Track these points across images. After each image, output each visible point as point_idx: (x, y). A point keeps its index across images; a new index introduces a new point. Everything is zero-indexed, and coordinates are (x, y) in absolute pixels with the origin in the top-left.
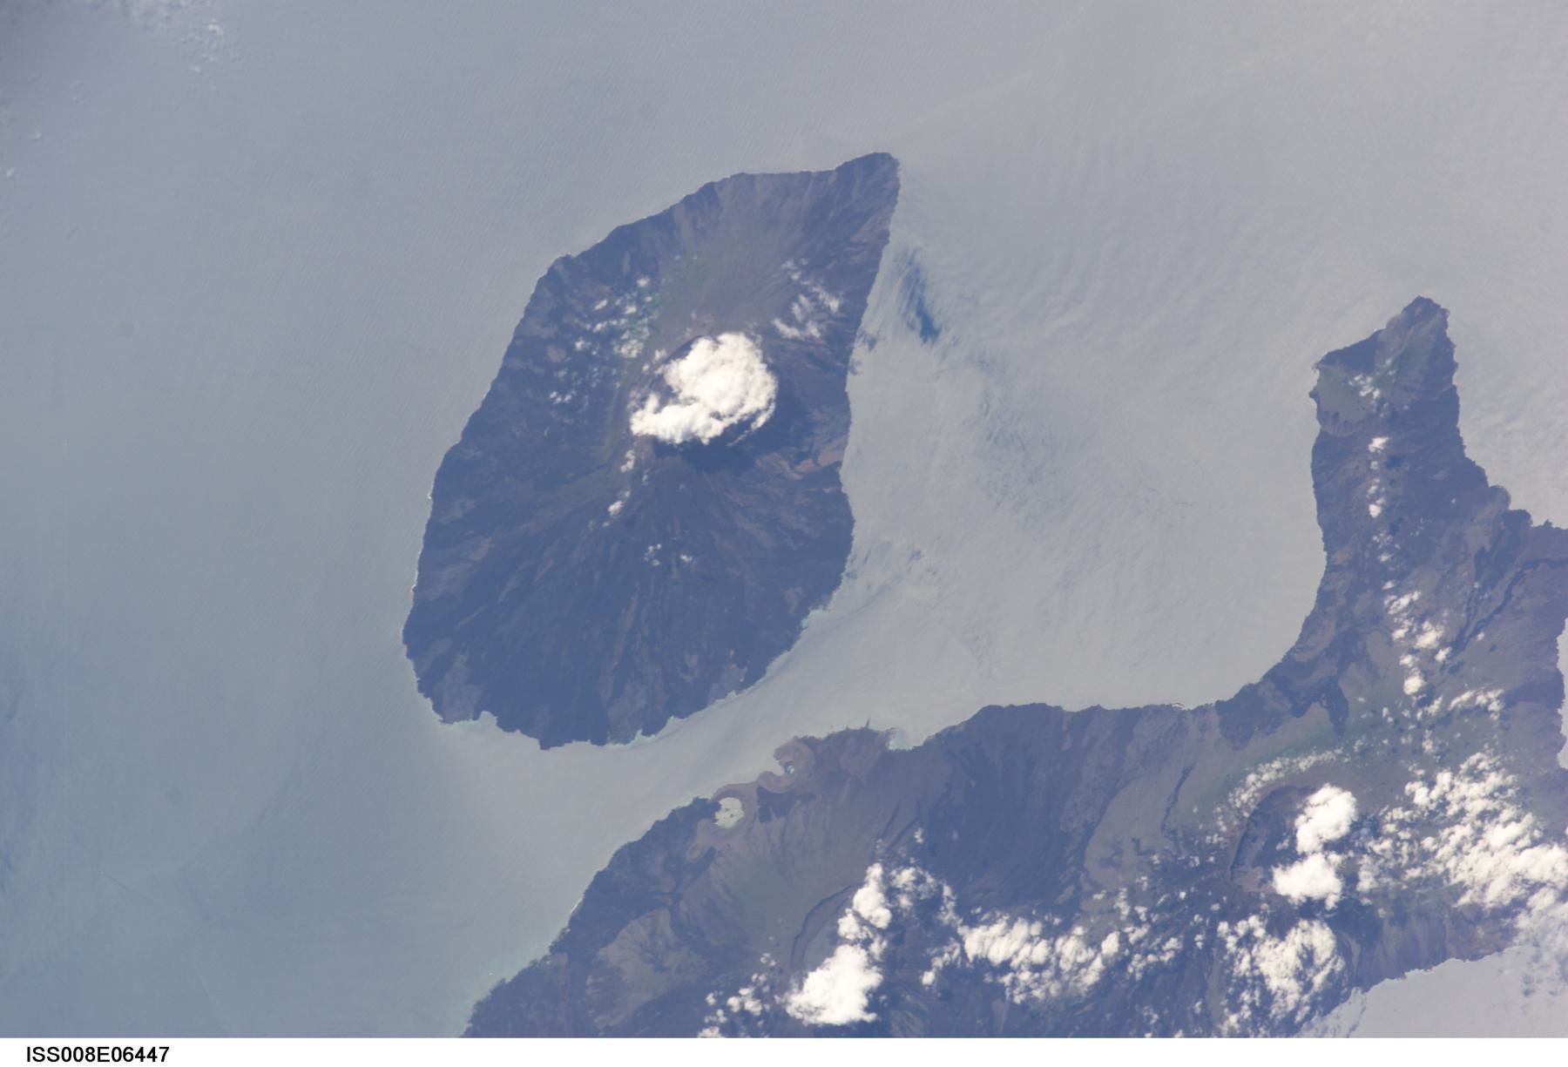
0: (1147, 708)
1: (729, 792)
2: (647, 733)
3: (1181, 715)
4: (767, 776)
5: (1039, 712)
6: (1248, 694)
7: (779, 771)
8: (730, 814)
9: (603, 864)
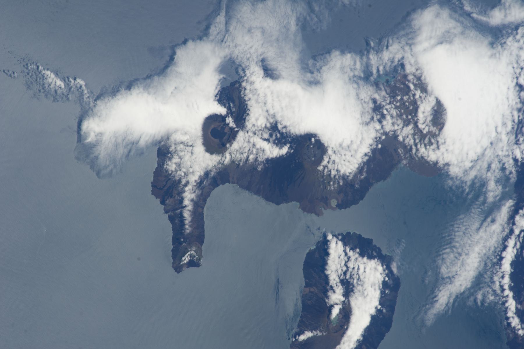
0: (244, 189)
1: (333, 209)
2: (350, 233)
3: (237, 184)
4: (325, 209)
5: (268, 198)
6: (223, 183)
7: (323, 209)
8: (334, 203)
9: (361, 201)
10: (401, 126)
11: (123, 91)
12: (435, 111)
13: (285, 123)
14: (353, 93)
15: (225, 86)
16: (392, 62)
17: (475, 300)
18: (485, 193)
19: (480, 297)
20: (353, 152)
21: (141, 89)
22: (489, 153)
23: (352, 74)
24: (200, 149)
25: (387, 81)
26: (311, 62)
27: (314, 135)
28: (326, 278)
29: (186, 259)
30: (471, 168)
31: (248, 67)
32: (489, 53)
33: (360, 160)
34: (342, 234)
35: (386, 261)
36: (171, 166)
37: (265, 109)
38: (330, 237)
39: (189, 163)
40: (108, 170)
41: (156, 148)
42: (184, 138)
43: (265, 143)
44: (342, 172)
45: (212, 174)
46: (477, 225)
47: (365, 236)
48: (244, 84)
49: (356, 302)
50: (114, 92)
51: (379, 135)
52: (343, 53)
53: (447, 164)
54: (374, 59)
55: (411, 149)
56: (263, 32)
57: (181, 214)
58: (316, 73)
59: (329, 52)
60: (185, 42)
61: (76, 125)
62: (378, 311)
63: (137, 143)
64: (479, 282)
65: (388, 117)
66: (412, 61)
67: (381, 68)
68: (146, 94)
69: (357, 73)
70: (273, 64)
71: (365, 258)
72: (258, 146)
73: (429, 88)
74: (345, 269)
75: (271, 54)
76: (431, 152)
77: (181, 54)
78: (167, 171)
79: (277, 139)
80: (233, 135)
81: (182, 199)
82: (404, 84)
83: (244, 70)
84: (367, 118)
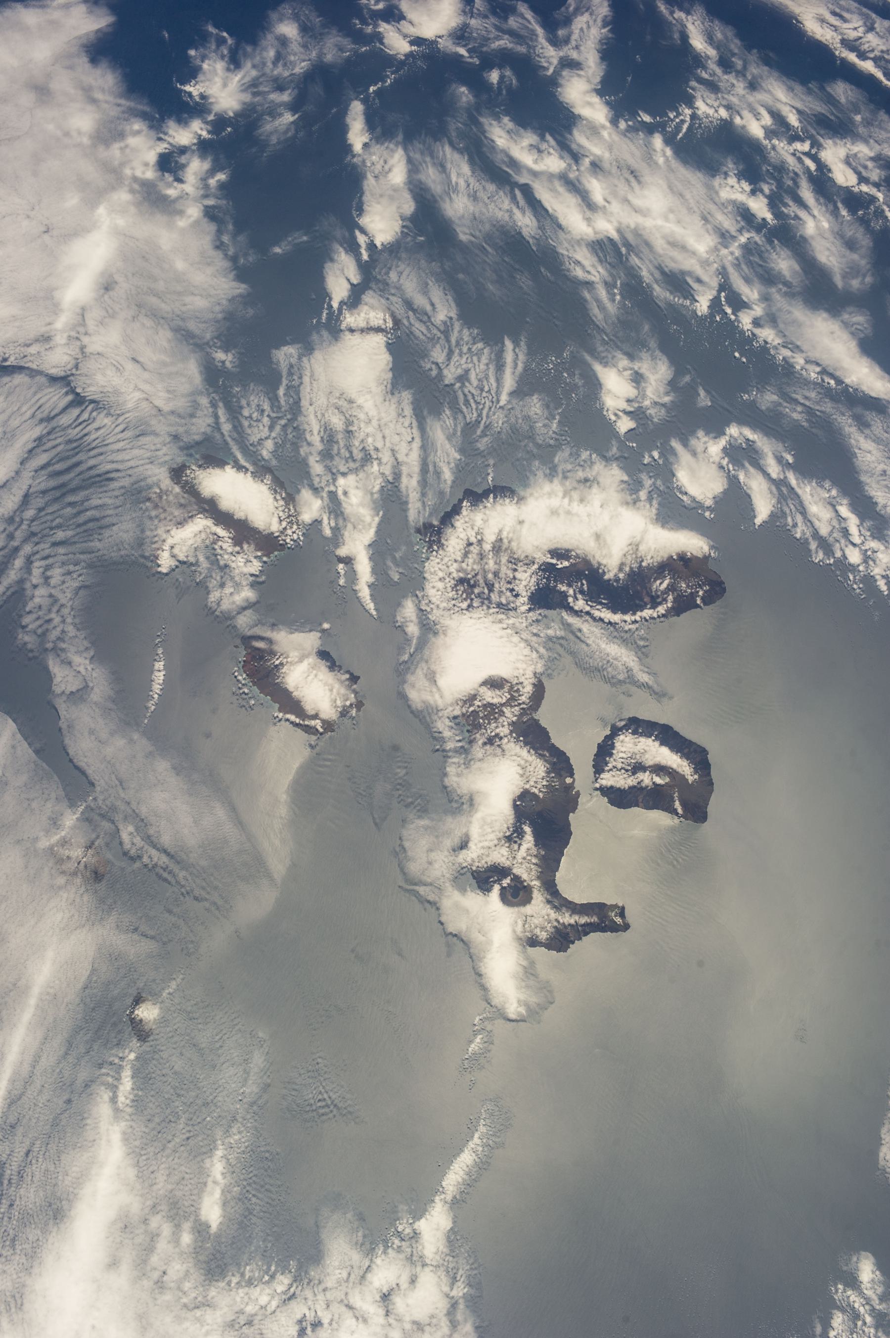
5: (567, 843)
6: (556, 885)
8: (569, 780)
10: (504, 718)
11: (483, 981)
12: (491, 686)
13: (505, 829)
14: (478, 764)
15: (476, 885)
16: (452, 728)
17: (644, 647)
18: (558, 638)
19: (642, 643)
20: (527, 764)
21: (482, 964)
22: (525, 635)
23: (463, 766)
24: (528, 909)
25: (468, 731)
26: (455, 805)
27: (515, 801)
28: (632, 788)
29: (618, 920)
30: (537, 652)
31: (460, 864)
32: (442, 636)
33: (534, 757)
34: (595, 773)
35: (615, 731)
36: (543, 936)
37: (493, 848)
38: (597, 785)
39: (541, 919)
40: (548, 994)
41: (528, 947)
42: (520, 923)
43: (522, 847)
44: (544, 774)
45: (548, 897)
46: (584, 646)
47: (595, 750)
48: (474, 868)
49: (649, 760)
50: (484, 988)
51: (512, 740)
52: (445, 775)
53: (535, 674)
54: (450, 745)
55: (522, 709)
56: (431, 850)
57: (582, 926)
58: (463, 800)
59: (445, 787)
60: (442, 924)
61: (512, 1023)
62: (657, 738)
63: (525, 967)
65: (498, 731)
66: (451, 709)
67: (458, 738)
68: (485, 960)
69: (462, 762)
70: (457, 841)
71: (614, 752)
72: (525, 855)
73: (472, 692)
74: (623, 771)
75: (448, 843)
76: (525, 690)
77: (451, 928)
78: (547, 939)
79: (517, 837)
80: (517, 879)
81: (570, 925)
82: (469, 716)
83: (462, 869)
84: (499, 751)
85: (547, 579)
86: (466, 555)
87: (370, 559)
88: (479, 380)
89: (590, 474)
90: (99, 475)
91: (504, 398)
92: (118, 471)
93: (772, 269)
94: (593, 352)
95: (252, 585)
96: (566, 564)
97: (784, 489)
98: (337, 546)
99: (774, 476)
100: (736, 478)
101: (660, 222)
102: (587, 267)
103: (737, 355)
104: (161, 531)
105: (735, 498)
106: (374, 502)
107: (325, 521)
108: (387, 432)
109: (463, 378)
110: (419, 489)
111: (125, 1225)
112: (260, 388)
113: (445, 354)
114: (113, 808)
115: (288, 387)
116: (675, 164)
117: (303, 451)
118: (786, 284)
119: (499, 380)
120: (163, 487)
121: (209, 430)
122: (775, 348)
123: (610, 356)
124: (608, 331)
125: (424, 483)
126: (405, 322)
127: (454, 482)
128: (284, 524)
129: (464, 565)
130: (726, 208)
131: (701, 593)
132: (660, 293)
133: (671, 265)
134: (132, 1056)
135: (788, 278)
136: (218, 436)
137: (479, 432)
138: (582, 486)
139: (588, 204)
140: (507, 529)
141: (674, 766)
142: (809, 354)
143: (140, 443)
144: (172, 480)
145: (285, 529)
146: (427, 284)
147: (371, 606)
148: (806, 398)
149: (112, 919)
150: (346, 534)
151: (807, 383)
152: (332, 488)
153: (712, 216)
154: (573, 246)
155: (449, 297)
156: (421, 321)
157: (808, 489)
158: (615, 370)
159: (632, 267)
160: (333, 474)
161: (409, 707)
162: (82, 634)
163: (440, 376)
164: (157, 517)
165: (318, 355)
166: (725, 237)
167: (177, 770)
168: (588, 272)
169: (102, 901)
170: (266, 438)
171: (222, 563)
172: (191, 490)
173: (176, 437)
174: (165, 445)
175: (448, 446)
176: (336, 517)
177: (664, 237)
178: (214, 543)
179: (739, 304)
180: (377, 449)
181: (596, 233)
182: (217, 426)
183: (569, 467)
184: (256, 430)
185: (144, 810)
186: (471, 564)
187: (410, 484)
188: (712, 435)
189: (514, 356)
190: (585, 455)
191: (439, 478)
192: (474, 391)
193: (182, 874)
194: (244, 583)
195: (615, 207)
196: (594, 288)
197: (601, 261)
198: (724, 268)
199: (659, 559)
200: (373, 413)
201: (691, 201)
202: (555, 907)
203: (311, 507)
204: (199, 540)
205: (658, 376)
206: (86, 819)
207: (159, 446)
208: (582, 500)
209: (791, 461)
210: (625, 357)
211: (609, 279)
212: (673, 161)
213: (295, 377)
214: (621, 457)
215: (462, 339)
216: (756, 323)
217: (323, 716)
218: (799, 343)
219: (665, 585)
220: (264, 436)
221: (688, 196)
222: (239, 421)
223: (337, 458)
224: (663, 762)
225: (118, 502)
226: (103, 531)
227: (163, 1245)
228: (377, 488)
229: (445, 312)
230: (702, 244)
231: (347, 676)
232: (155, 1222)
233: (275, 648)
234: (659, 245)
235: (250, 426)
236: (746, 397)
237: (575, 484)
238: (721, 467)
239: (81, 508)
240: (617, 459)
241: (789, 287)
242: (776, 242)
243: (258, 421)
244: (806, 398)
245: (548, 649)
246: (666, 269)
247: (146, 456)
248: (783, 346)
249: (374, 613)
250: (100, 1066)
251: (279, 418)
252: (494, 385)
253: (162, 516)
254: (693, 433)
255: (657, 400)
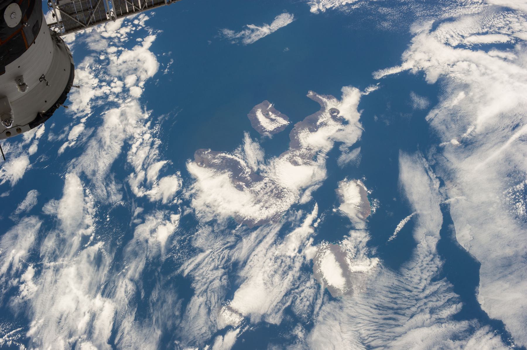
14: (319, 146)
22: (274, 171)
24: (334, 107)
27: (316, 131)
42: (339, 106)
49: (268, 120)
54: (323, 155)
64: (243, 150)
70: (341, 132)
75: (343, 133)
80: (331, 114)
84: (310, 146)
85: (251, 183)
86: (272, 204)
87: (303, 222)
88: (210, 264)
89: (204, 208)
90: (379, 310)
91: (208, 252)
92: (371, 307)
93: (57, 244)
94: (160, 250)
95: (349, 236)
96: (241, 183)
97: (145, 167)
98: (312, 234)
99: (144, 172)
100: (157, 179)
101: (75, 291)
102: (125, 288)
103: (108, 219)
104: (370, 274)
105: (162, 174)
106: (287, 241)
107: (309, 244)
108: (261, 263)
109: (216, 268)
110: (268, 236)
111: (485, 104)
112: (295, 310)
113: (214, 282)
114: (437, 194)
115: (284, 304)
116: (37, 315)
117: (298, 275)
118: (58, 236)
119: (204, 260)
120: (359, 291)
121: (326, 304)
122: (92, 214)
123: (154, 245)
124: (144, 255)
125: (264, 237)
126: (216, 306)
127: (253, 231)
128: (324, 251)
129: (275, 202)
130: (42, 282)
131: (207, 152)
132: (108, 260)
133: (92, 269)
134: (465, 135)
135: (55, 237)
136: (325, 300)
137: (229, 245)
138: (211, 205)
139: (94, 317)
140: (250, 206)
141: (262, 115)
142: (83, 205)
143: (356, 314)
144: (353, 292)
145: (325, 249)
146: (194, 318)
147: (316, 207)
148: (102, 191)
149: (453, 167)
150: (306, 235)
151: (96, 196)
152: (298, 254)
153: (52, 281)
154: (120, 301)
155: (190, 306)
156: (210, 302)
157: (138, 162)
158: (158, 239)
159: (108, 277)
160: (293, 260)
161: (327, 172)
162: (419, 253)
163: (224, 274)
164: (368, 280)
165: (262, 312)
166: (57, 270)
167: (411, 194)
168: (126, 285)
169: (454, 173)
170: (307, 288)
171: (356, 250)
172: (348, 283)
173: (341, 308)
174: (347, 307)
175: (244, 246)
176: (304, 244)
177: (81, 283)
178: (354, 258)
179: (85, 239)
180: (271, 259)
181: (105, 301)
182: (323, 304)
183: (209, 214)
184: (309, 293)
185: (428, 188)
186: (272, 200)
187: (270, 239)
188: (149, 197)
189: (187, 267)
190: (199, 215)
191: (257, 236)
192: (216, 260)
193: (427, 166)
194: (352, 239)
195: (85, 308)
196: (131, 276)
197: (116, 287)
198: (73, 256)
199: (210, 169)
200: (261, 274)
201: (52, 293)
202: (326, 105)
203: (310, 251)
204: (358, 263)
205: (145, 228)
206: (447, 198)
207: (350, 308)
208: (216, 201)
209: (133, 174)
210: (149, 242)
211: (122, 277)
212: (37, 317)
213: (278, 307)
214: (187, 207)
215: (202, 285)
216: (88, 227)
217: (355, 184)
218: (82, 211)
219: (216, 160)
220: (308, 290)
221: (51, 296)
222: (313, 301)
223: (288, 264)
224: (264, 117)
225: (378, 294)
226: (390, 286)
227: (478, 96)
228: (282, 245)
229: (198, 300)
230: (70, 272)
231: (339, 191)
232: (477, 101)
233: (356, 212)
234: (86, 281)
235: (310, 296)
236: (122, 203)
237: (213, 207)
238: (158, 185)
239: (393, 300)
240: (190, 207)
241: (59, 234)
242: (41, 255)
243: (306, 297)
244: (102, 191)
245: (269, 163)
246: (96, 268)
247: (357, 307)
248: (88, 212)
249: (316, 205)
250: (474, 137)
251: (297, 293)
252: (207, 259)
253: (366, 279)
254: (155, 202)
255: (154, 220)
